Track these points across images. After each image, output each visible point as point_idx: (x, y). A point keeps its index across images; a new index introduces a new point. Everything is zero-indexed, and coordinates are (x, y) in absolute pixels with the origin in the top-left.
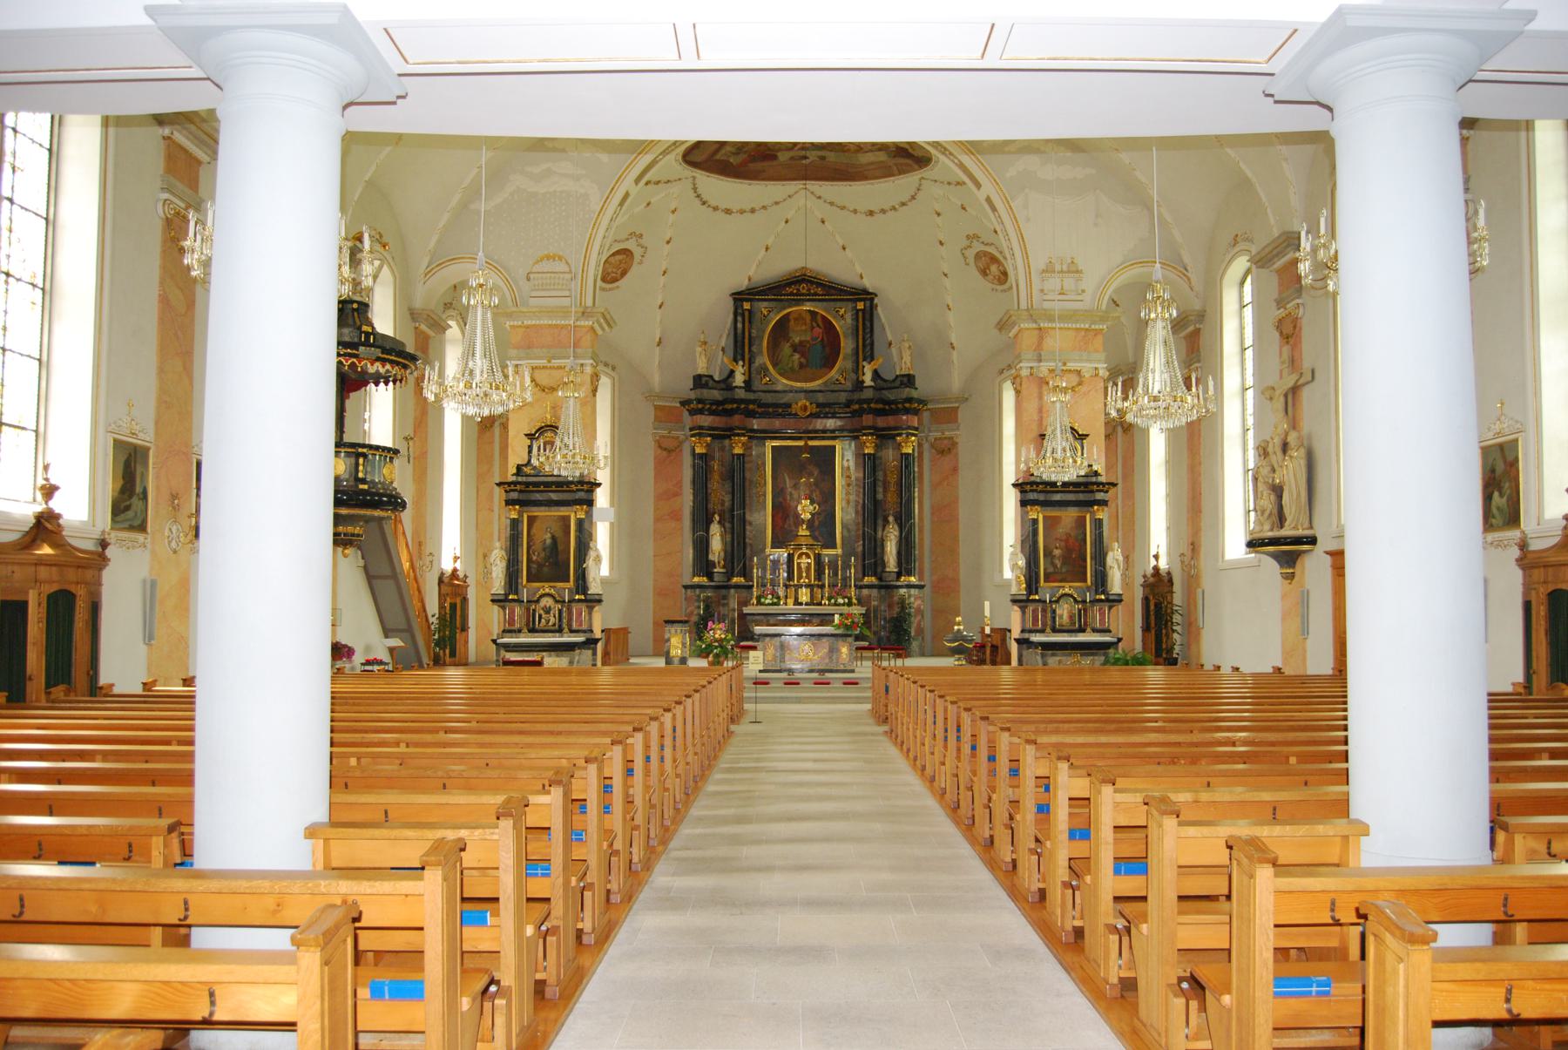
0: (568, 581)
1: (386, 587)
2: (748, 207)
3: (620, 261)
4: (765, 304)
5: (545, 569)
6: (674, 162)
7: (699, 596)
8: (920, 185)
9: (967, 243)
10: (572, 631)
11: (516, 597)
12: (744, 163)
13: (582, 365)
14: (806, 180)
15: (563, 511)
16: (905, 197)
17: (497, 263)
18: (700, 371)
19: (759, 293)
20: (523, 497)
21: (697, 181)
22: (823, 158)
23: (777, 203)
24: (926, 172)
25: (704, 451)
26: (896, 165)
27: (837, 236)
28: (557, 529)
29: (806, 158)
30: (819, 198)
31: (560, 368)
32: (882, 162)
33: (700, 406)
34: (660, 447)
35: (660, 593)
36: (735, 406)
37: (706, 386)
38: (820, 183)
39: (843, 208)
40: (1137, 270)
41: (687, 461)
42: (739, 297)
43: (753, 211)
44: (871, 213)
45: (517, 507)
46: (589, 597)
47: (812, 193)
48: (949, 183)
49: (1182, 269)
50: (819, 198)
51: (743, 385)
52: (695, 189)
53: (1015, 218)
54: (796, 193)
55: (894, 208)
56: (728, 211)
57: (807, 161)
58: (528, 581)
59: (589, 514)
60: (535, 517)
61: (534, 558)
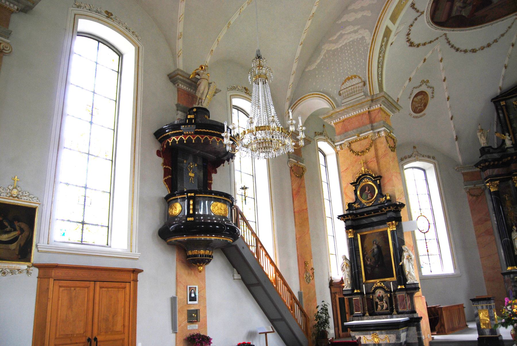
0: (393, 277)
1: (258, 290)
3: (421, 99)
4: (515, 99)
5: (377, 270)
6: (427, 24)
7: (513, 279)
10: (399, 313)
11: (359, 291)
13: (378, 132)
15: (382, 228)
17: (322, 93)
18: (482, 146)
19: (509, 94)
20: (355, 224)
21: (448, 36)
25: (496, 189)
28: (379, 240)
31: (365, 138)
33: (487, 164)
34: (470, 195)
35: (489, 279)
36: (509, 158)
37: (489, 152)
41: (488, 197)
42: (496, 100)
43: (489, 45)
45: (350, 230)
46: (407, 287)
51: (511, 146)
52: (449, 42)
56: (474, 51)
58: (367, 279)
59: (399, 227)
60: (366, 234)
61: (368, 263)
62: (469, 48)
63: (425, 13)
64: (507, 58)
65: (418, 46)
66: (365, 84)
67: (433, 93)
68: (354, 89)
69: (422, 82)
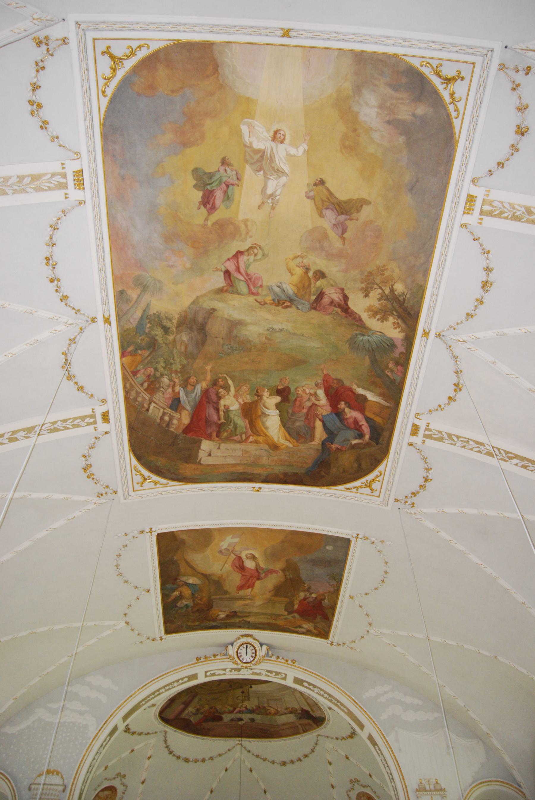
2: (200, 758)
3: (107, 796)
6: (153, 717)
8: (317, 740)
9: (349, 786)
12: (199, 723)
14: (241, 737)
16: (307, 751)
22: (253, 720)
23: (220, 755)
24: (322, 730)
26: (301, 725)
27: (261, 782)
29: (241, 719)
30: (249, 751)
32: (293, 723)
38: (251, 740)
39: (265, 760)
40: (485, 788)
43: (204, 760)
44: (284, 764)
47: (245, 748)
48: (337, 739)
49: (518, 787)
50: (249, 751)
52: (165, 741)
53: (391, 749)
54: (234, 747)
55: (300, 760)
56: (187, 760)
57: (243, 722)
62: (183, 756)
63: (156, 707)
64: (216, 782)
65: (134, 733)
66: (64, 791)
67: (124, 793)
68: (50, 789)
69: (117, 775)
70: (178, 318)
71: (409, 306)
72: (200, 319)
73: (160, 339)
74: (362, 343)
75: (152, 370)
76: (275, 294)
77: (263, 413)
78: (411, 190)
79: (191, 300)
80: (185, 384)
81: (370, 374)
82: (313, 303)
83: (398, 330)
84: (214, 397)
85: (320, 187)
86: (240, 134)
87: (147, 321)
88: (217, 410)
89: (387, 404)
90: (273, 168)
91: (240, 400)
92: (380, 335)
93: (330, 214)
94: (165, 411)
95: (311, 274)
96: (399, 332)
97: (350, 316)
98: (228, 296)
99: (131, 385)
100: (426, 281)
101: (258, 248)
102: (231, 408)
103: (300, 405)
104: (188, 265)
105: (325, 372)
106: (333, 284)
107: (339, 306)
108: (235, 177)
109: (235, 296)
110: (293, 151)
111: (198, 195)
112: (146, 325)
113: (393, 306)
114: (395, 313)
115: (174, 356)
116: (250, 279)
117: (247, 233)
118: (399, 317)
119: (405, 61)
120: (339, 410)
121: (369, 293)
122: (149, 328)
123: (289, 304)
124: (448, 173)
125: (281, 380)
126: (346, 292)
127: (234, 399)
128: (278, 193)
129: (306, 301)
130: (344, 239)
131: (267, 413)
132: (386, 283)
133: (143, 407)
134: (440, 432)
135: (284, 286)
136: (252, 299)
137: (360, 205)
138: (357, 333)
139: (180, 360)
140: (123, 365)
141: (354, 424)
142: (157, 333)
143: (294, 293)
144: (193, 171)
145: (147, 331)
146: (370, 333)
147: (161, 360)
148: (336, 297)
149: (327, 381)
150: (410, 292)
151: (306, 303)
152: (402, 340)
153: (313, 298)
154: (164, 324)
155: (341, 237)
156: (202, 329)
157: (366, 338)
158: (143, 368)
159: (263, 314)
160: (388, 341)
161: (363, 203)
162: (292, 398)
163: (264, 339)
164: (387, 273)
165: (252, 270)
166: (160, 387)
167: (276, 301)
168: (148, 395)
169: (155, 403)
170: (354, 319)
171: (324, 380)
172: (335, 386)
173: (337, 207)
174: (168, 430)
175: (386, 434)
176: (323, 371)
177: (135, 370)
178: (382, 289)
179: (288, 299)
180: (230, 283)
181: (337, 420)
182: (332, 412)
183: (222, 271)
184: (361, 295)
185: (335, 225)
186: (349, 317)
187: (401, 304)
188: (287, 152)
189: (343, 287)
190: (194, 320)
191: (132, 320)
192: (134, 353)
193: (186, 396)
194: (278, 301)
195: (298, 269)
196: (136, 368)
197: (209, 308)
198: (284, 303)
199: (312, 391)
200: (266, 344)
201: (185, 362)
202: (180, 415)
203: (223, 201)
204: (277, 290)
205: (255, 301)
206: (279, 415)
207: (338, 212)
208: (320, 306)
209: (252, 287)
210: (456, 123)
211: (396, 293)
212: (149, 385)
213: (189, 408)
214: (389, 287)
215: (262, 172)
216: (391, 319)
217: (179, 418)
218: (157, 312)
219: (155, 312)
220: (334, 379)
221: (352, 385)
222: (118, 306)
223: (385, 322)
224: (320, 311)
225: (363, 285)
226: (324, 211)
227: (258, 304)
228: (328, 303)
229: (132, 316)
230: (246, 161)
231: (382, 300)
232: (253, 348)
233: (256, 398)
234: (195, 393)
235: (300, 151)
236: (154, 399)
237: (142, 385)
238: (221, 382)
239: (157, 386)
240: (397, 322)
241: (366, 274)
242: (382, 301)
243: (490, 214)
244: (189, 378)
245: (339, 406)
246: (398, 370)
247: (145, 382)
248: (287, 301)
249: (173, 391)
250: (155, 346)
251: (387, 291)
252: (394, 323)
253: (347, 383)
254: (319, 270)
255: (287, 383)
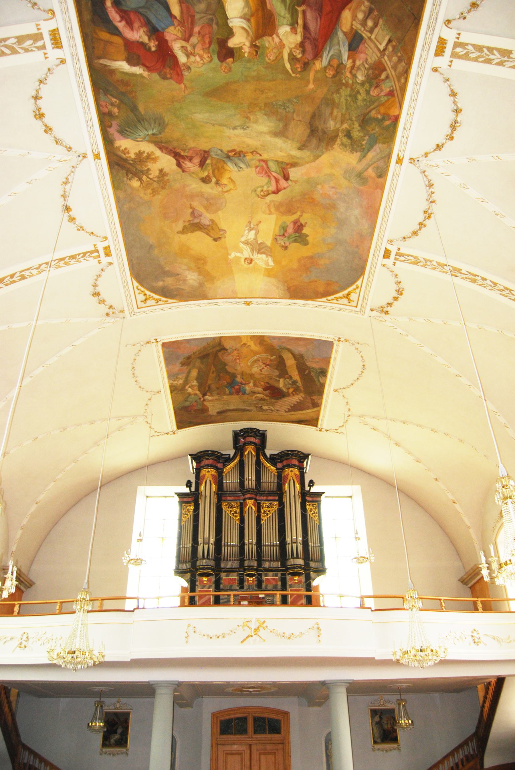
70: (334, 144)
71: (121, 171)
72: (314, 141)
73: (356, 125)
74: (152, 126)
75: (371, 93)
76: (243, 162)
77: (248, 20)
78: (151, 246)
79: (320, 159)
80: (339, 69)
81: (134, 94)
82: (208, 157)
83: (123, 148)
84: (308, 46)
85: (216, 236)
86: (275, 261)
87: (364, 147)
88: (305, 27)
89: (102, 61)
90: (251, 245)
91: (277, 40)
92: (137, 138)
93: (205, 221)
94: (369, 35)
95: (214, 180)
96: (121, 147)
97: (171, 150)
98: (286, 160)
99: (399, 81)
100: (115, 194)
101: (260, 196)
102: (288, 28)
103: (203, 36)
104: (319, 187)
105: (182, 86)
106: (192, 174)
107: (183, 157)
108: (278, 240)
109: (280, 160)
110: (238, 254)
111: (306, 231)
112: (366, 144)
113: (135, 167)
114: (131, 162)
115: (346, 105)
116: (266, 173)
117: (269, 206)
118: (126, 159)
119: (177, 300)
120: (154, 37)
121: (159, 174)
122: (364, 140)
123: (230, 154)
124: (130, 261)
125: (230, 70)
126: (180, 170)
127: (284, 42)
128: (247, 231)
129: (215, 158)
130: (191, 207)
131: (244, 21)
132: (148, 184)
133: (394, 47)
134: (26, 50)
135: (236, 169)
136: (265, 157)
137: (185, 230)
138: (160, 135)
139: (340, 99)
140: (401, 107)
141: (131, 20)
142: (358, 133)
143: (226, 164)
144: (308, 244)
145: (367, 137)
146: (147, 138)
147: (360, 103)
148: (188, 164)
149: (178, 74)
150: (125, 182)
151: (214, 156)
152: (115, 140)
153: (208, 161)
154: (349, 141)
155: (194, 209)
156: (313, 131)
157: (150, 132)
158: (381, 96)
159: (253, 143)
160: (128, 135)
161: (184, 231)
162: (215, 47)
163: (252, 118)
164: (149, 191)
165: (265, 180)
166: (368, 69)
167: (242, 156)
168: (384, 62)
169: (379, 49)
170: (167, 148)
171: (182, 75)
172: (168, 71)
173: (202, 227)
174: (372, 3)
175: (87, 16)
176: (185, 87)
177: (390, 97)
178: (150, 178)
179: (232, 158)
180: (284, 170)
181: (154, 21)
182: (163, 33)
183: (291, 180)
184: (166, 170)
185: (201, 216)
186: (172, 149)
187: (128, 171)
188: (242, 254)
189: (184, 173)
190: (320, 140)
191: (378, 151)
192: (386, 116)
193: (340, 51)
194: (240, 156)
195: (226, 183)
196: (388, 100)
197: (304, 151)
198: (234, 155)
199: (192, 59)
200: (250, 113)
201: (336, 96)
202: (352, 25)
203: (287, 226)
204: (242, 165)
205: (262, 155)
206: (228, 18)
207: (200, 224)
208: (201, 154)
209: (265, 166)
210: (136, 284)
211: (136, 179)
212: (380, 75)
213: (340, 35)
214: (143, 181)
215: (259, 242)
216: (133, 156)
217: (355, 20)
218: (353, 153)
219: (355, 153)
220: (171, 78)
221: (148, 75)
222: (387, 167)
223: (137, 152)
224: (201, 150)
225: (166, 178)
226: (210, 223)
227: (259, 152)
228: (194, 159)
229: (377, 154)
230: (270, 248)
231: (146, 170)
232: (263, 107)
233: (257, 43)
234: (330, 55)
235: (233, 255)
236: (379, 55)
237: (387, 77)
238: (298, 66)
239: (371, 72)
240: (127, 155)
241: (167, 187)
242: (146, 168)
243: (92, 252)
244: (334, 76)
245: (157, 43)
246: (107, 107)
247: (383, 80)
248: (232, 156)
249: (354, 62)
250: (363, 120)
251: (144, 178)
252: (128, 153)
253: (155, 76)
254: (207, 183)
255: (223, 67)
